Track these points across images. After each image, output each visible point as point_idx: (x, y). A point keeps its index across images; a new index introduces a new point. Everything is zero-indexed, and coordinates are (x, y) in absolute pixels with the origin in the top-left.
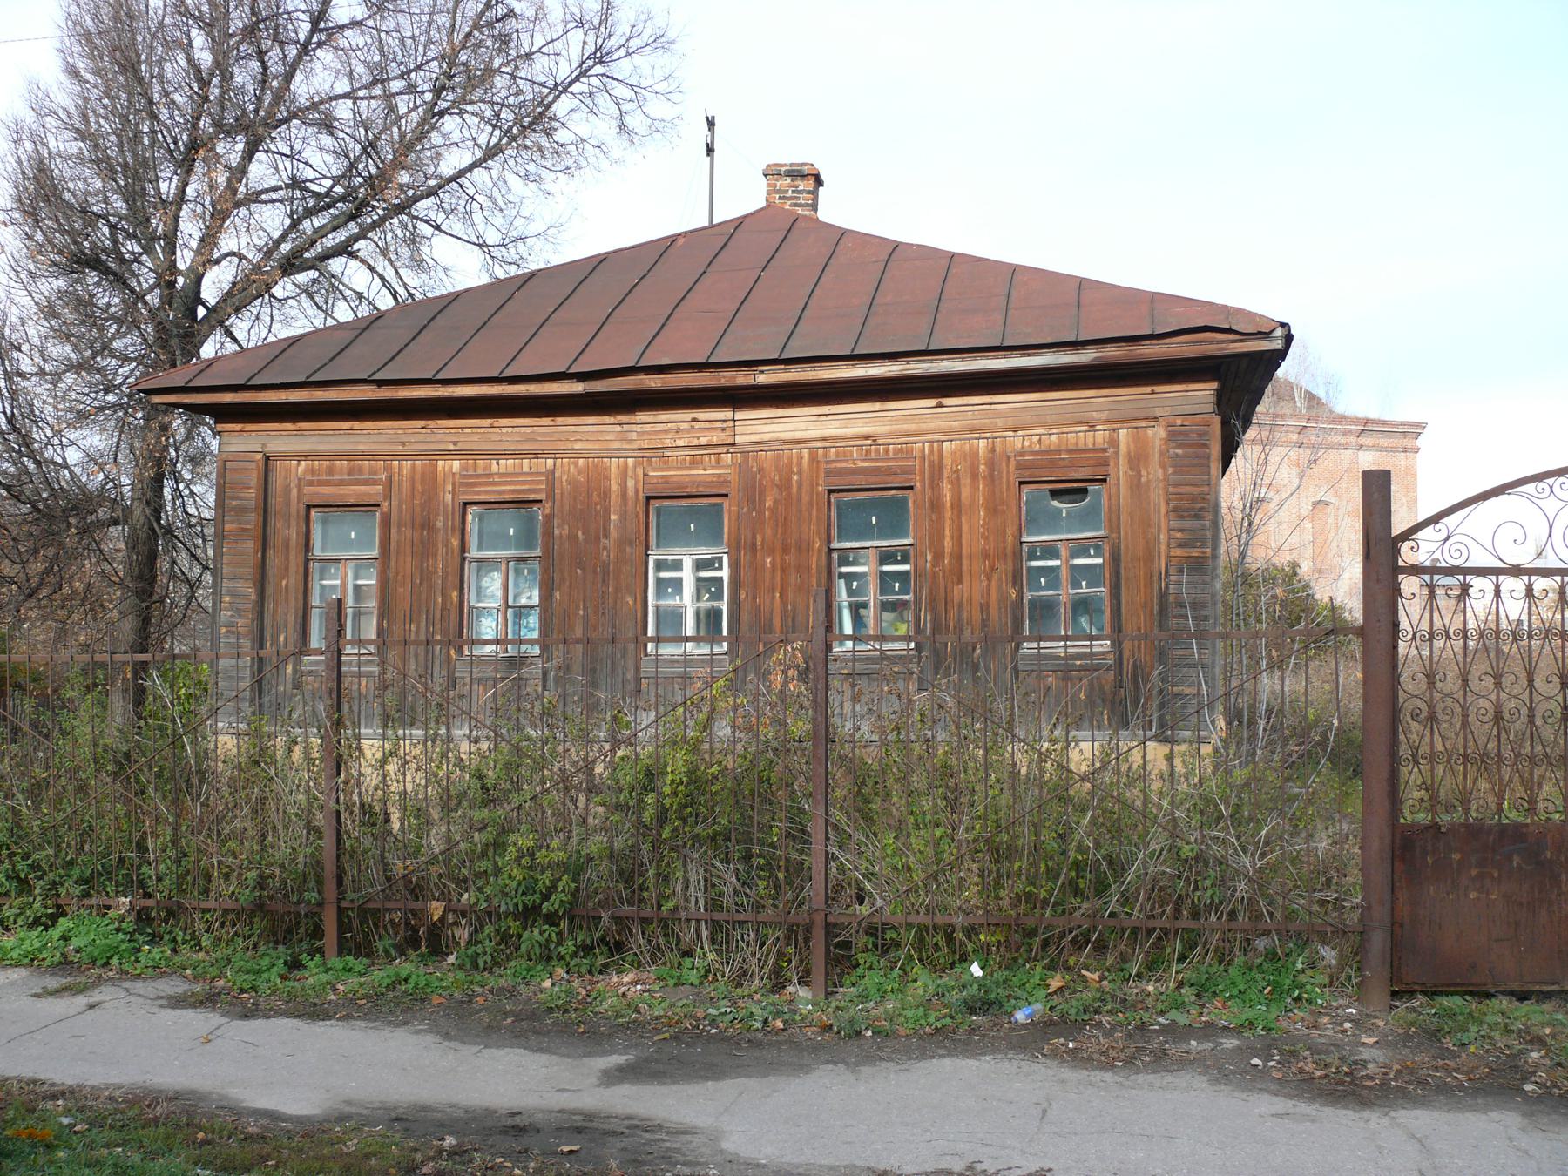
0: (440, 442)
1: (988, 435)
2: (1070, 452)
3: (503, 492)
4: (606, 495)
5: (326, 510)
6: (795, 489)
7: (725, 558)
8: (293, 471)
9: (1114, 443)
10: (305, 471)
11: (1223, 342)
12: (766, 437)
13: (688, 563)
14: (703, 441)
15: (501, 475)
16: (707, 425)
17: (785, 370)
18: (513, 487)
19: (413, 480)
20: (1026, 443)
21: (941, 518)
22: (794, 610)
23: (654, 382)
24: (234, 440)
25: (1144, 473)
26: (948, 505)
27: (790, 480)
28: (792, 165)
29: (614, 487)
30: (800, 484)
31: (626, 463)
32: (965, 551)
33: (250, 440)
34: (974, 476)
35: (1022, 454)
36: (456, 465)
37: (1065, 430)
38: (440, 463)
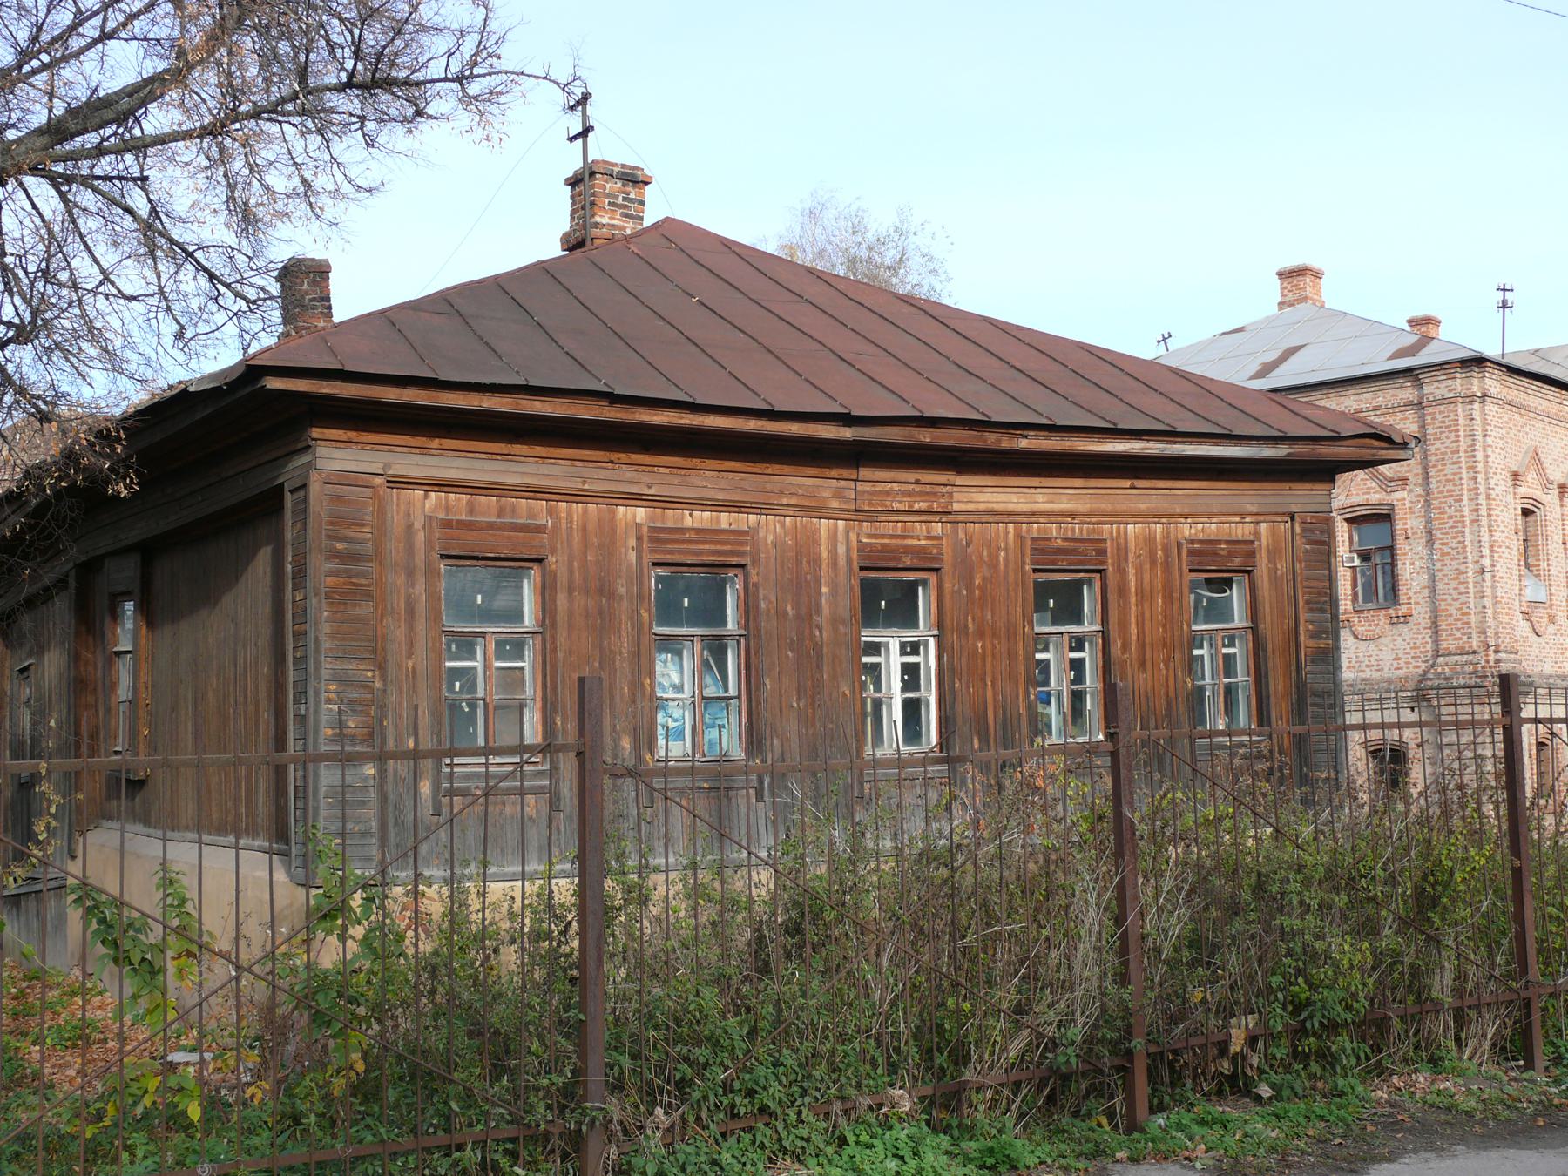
0: (630, 482)
1: (1164, 520)
2: (1227, 542)
3: (700, 553)
4: (815, 561)
5: (462, 563)
6: (1002, 567)
7: (932, 643)
8: (418, 505)
9: (1257, 534)
10: (437, 506)
11: (1376, 448)
12: (982, 507)
13: (894, 646)
14: (923, 506)
15: (698, 531)
16: (928, 489)
17: (1047, 437)
18: (712, 547)
19: (584, 529)
20: (1193, 531)
21: (1127, 602)
22: (1004, 700)
23: (926, 436)
24: (338, 453)
25: (1279, 566)
26: (1133, 589)
27: (997, 556)
28: (623, 166)
29: (825, 554)
30: (1006, 560)
31: (836, 526)
32: (1148, 640)
33: (364, 455)
34: (1153, 563)
35: (1192, 542)
36: (641, 513)
37: (1224, 519)
38: (621, 509)
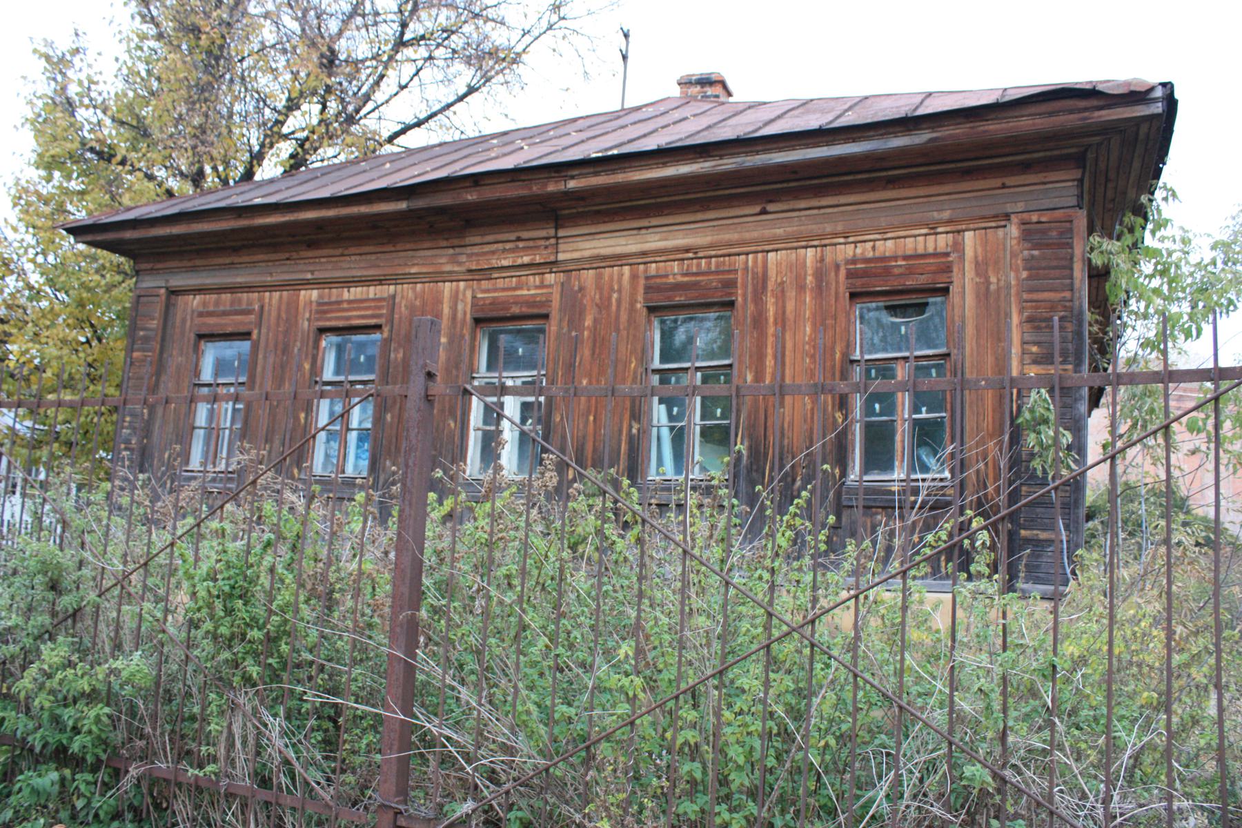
1: (815, 243)
2: (906, 258)
6: (614, 308)
9: (958, 247)
12: (587, 254)
14: (526, 260)
15: (349, 302)
16: (531, 244)
19: (279, 309)
20: (859, 251)
25: (993, 279)
26: (771, 320)
27: (610, 298)
29: (446, 310)
30: (619, 301)
31: (458, 287)
34: (801, 288)
